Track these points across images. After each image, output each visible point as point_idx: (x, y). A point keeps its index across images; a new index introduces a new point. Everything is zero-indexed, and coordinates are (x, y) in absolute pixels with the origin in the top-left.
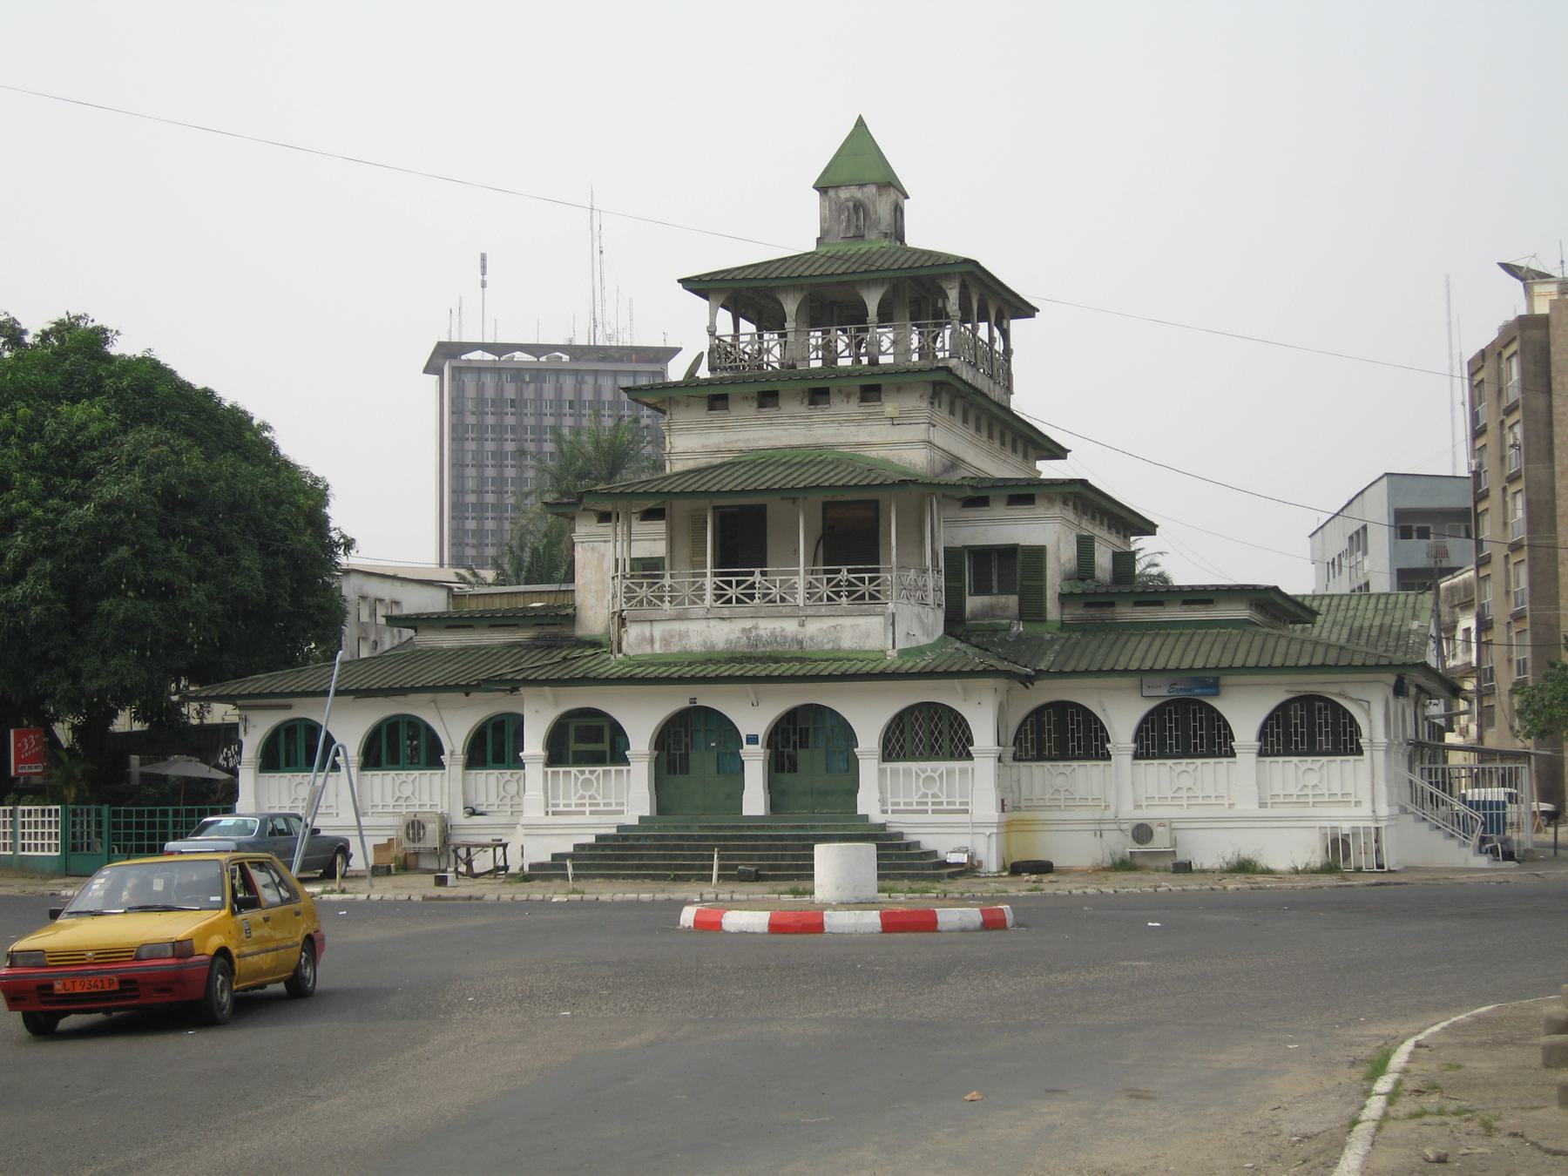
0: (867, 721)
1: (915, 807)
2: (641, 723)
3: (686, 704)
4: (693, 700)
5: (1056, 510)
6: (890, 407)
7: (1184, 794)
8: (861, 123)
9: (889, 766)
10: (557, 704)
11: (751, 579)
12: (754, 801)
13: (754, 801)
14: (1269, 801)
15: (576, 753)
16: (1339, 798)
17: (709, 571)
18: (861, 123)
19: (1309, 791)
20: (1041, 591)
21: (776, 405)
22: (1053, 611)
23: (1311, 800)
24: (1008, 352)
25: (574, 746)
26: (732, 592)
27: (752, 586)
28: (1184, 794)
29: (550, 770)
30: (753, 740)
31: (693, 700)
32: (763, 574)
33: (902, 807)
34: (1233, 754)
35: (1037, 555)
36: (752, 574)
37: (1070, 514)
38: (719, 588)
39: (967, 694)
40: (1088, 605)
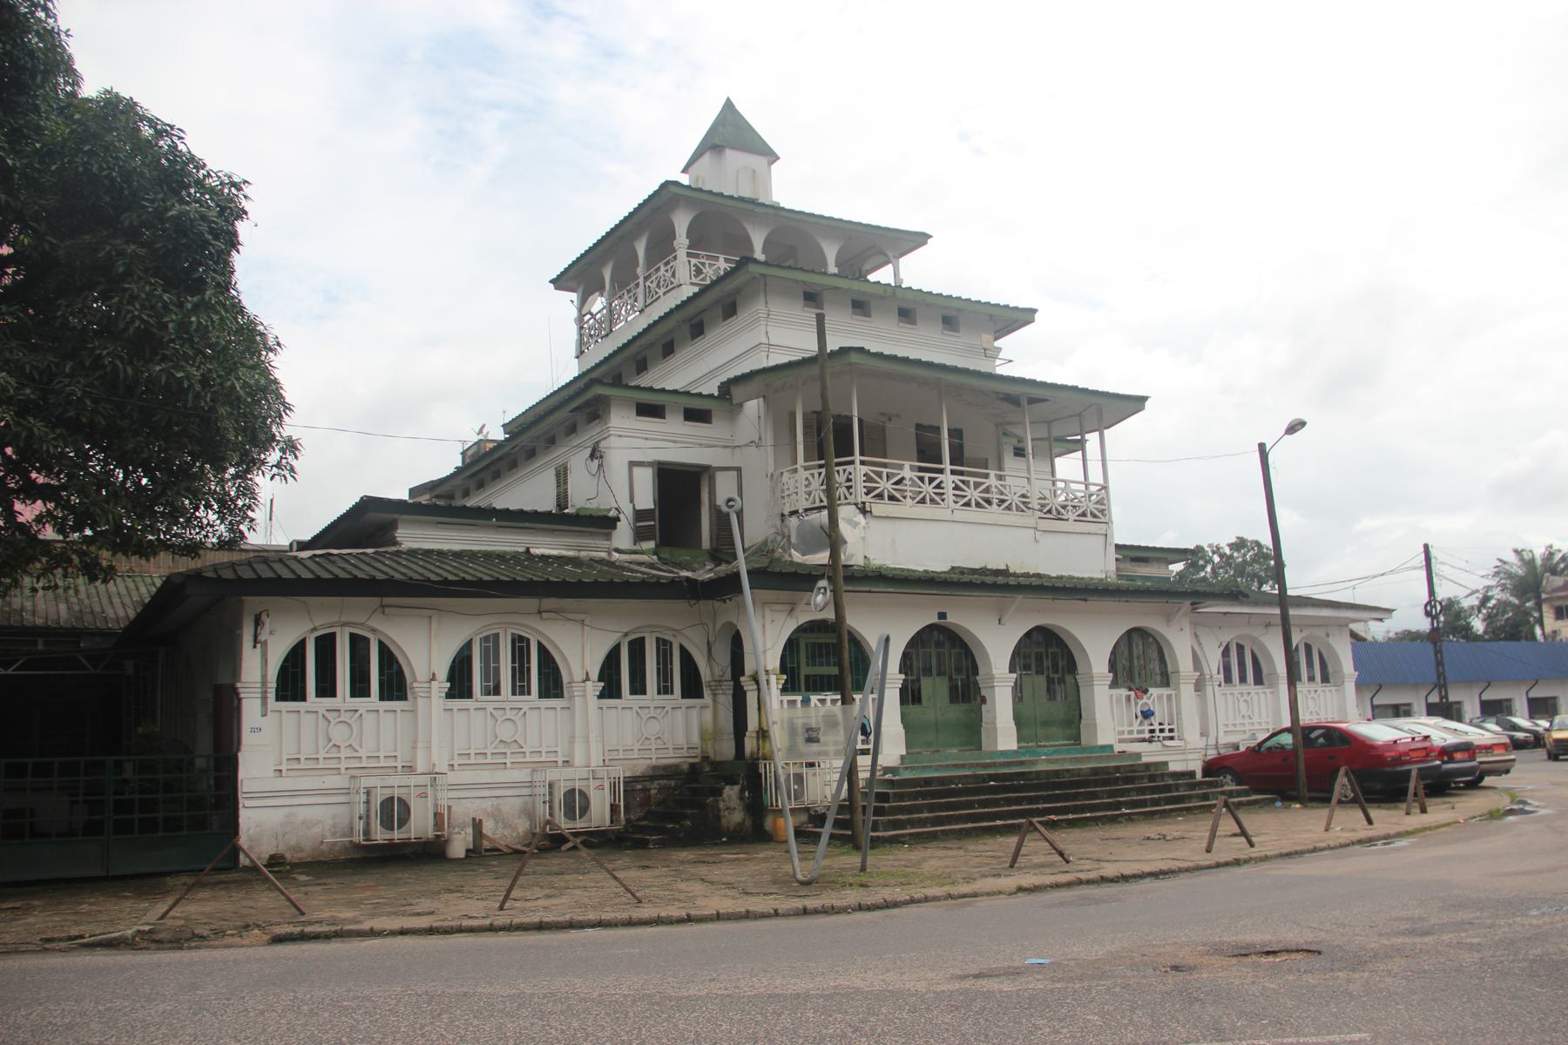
0: (1095, 642)
1: (1136, 736)
3: (933, 619)
4: (942, 616)
9: (1116, 692)
11: (988, 482)
12: (1003, 734)
13: (1003, 734)
15: (807, 677)
17: (947, 466)
21: (868, 315)
25: (805, 670)
26: (973, 494)
27: (987, 490)
28: (1247, 721)
29: (786, 698)
31: (942, 616)
32: (1000, 478)
33: (1126, 736)
36: (986, 476)
38: (956, 488)
39: (1169, 619)
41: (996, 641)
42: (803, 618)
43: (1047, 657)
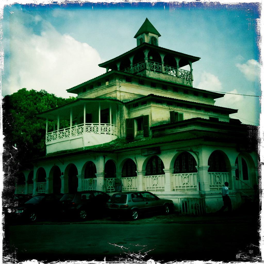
2: (48, 170)
3: (53, 165)
4: (55, 164)
5: (152, 105)
6: (107, 83)
7: (155, 186)
8: (147, 20)
10: (37, 167)
14: (175, 189)
16: (193, 188)
18: (147, 20)
19: (185, 185)
20: (147, 127)
22: (150, 133)
23: (186, 188)
24: (192, 70)
30: (63, 174)
31: (55, 164)
34: (164, 173)
35: (147, 117)
37: (165, 106)
40: (159, 130)
41: (63, 168)
42: (39, 167)
43: (72, 170)
